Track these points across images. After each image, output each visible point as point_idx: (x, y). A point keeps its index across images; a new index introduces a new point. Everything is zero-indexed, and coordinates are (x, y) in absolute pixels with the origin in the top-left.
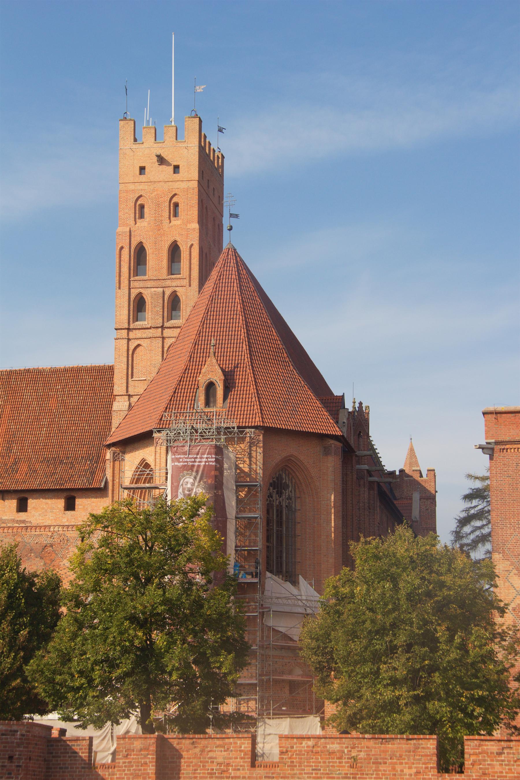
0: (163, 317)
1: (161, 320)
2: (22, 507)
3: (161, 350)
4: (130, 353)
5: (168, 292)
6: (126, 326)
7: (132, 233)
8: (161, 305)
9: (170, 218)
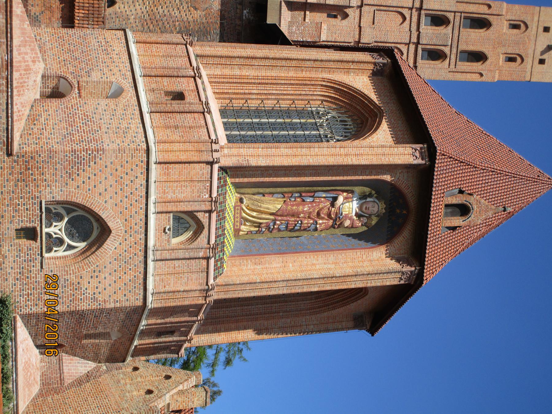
0: (426, 45)
1: (424, 42)
3: (399, 41)
4: (400, 10)
5: (447, 50)
6: (425, 7)
7: (499, 17)
8: (437, 43)
9: (505, 54)
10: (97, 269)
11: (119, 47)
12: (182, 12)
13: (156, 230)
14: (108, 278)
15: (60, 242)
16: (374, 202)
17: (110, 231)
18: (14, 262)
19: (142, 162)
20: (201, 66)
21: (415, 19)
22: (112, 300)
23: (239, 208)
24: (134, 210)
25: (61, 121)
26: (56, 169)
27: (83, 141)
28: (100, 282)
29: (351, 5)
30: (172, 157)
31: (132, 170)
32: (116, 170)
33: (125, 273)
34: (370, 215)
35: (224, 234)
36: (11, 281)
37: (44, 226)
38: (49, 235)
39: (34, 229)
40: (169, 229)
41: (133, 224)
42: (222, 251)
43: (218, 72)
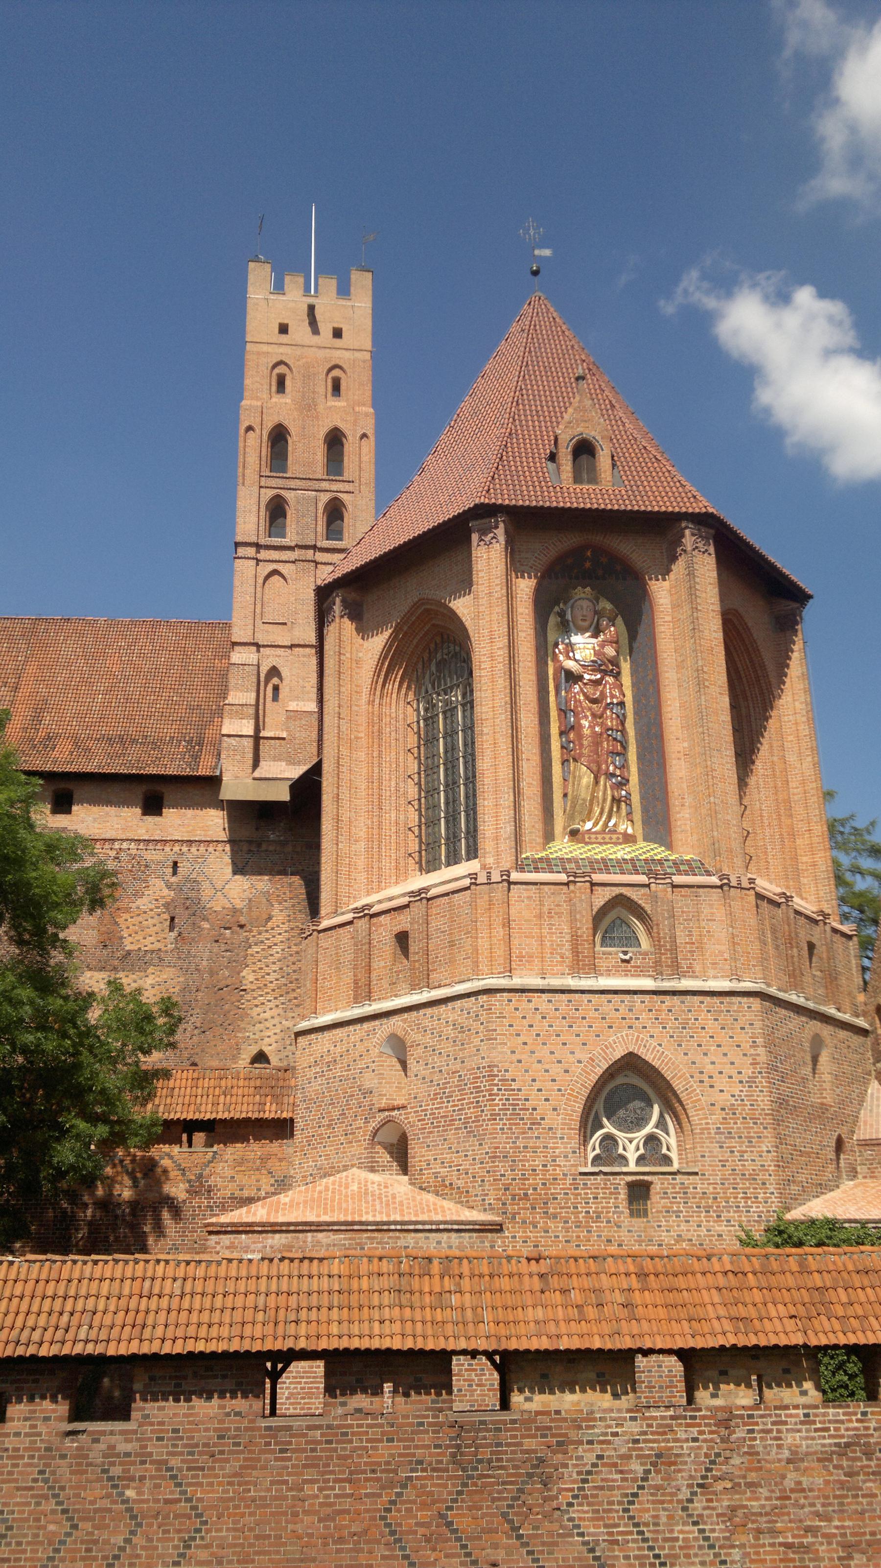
5: (325, 498)
6: (253, 539)
10: (697, 1077)
12: (275, 940)
13: (626, 975)
14: (714, 1059)
16: (572, 607)
17: (631, 1054)
18: (688, 1221)
19: (510, 1001)
20: (351, 907)
22: (752, 1051)
23: (587, 836)
24: (592, 1014)
25: (445, 1140)
26: (525, 1147)
27: (478, 1102)
28: (721, 1073)
29: (255, 663)
30: (500, 952)
31: (524, 1017)
32: (525, 1044)
33: (703, 1028)
34: (596, 612)
35: (632, 859)
36: (722, 1228)
37: (625, 1169)
38: (640, 1160)
39: (631, 1186)
40: (625, 953)
41: (618, 1015)
42: (660, 862)
43: (362, 877)
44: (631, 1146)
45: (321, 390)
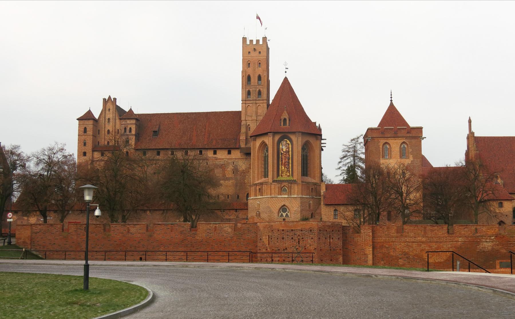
2: (215, 153)
5: (258, 90)
11: (251, 201)
15: (287, 214)
21: (249, 102)
44: (284, 214)
45: (257, 66)
